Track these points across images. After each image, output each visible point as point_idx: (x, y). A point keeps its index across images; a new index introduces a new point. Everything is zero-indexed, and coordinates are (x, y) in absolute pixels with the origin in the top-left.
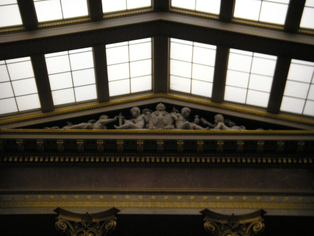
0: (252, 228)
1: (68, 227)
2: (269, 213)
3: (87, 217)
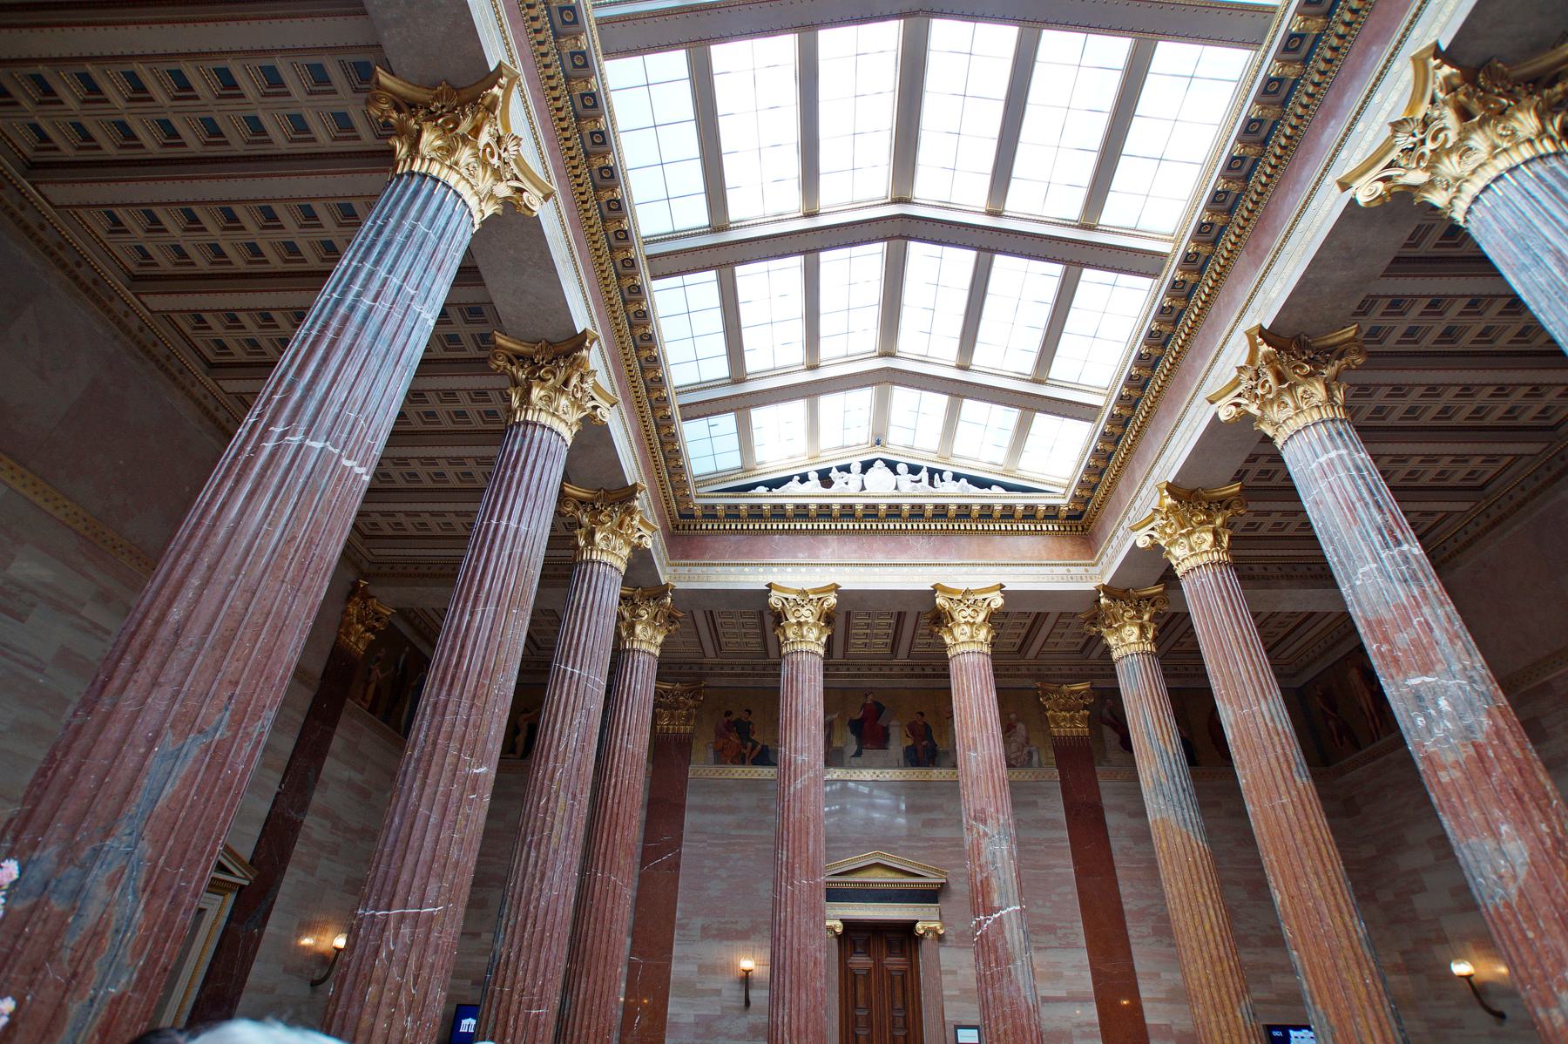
3: (804, 593)
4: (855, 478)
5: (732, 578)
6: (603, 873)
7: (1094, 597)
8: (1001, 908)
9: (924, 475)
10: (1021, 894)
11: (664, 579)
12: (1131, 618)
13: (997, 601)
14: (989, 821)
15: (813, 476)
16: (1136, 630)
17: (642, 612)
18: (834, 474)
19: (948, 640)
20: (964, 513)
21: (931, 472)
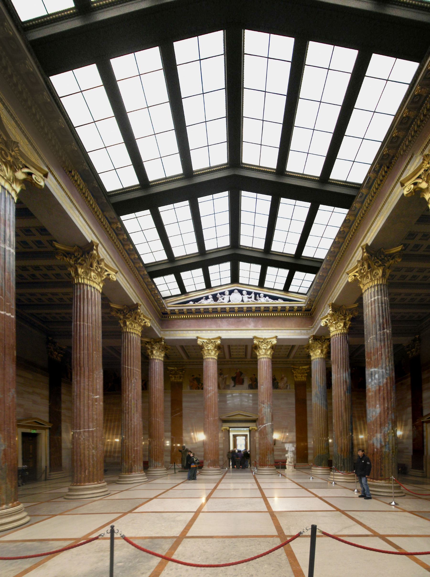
0: (272, 343)
1: (202, 343)
2: (279, 337)
3: (209, 340)
4: (226, 298)
5: (184, 335)
6: (154, 418)
7: (308, 340)
8: (266, 424)
9: (253, 295)
10: (272, 420)
11: (160, 336)
12: (319, 347)
13: (274, 342)
14: (265, 403)
15: (210, 297)
16: (320, 351)
17: (155, 347)
18: (219, 295)
19: (258, 354)
20: (267, 310)
21: (256, 294)
